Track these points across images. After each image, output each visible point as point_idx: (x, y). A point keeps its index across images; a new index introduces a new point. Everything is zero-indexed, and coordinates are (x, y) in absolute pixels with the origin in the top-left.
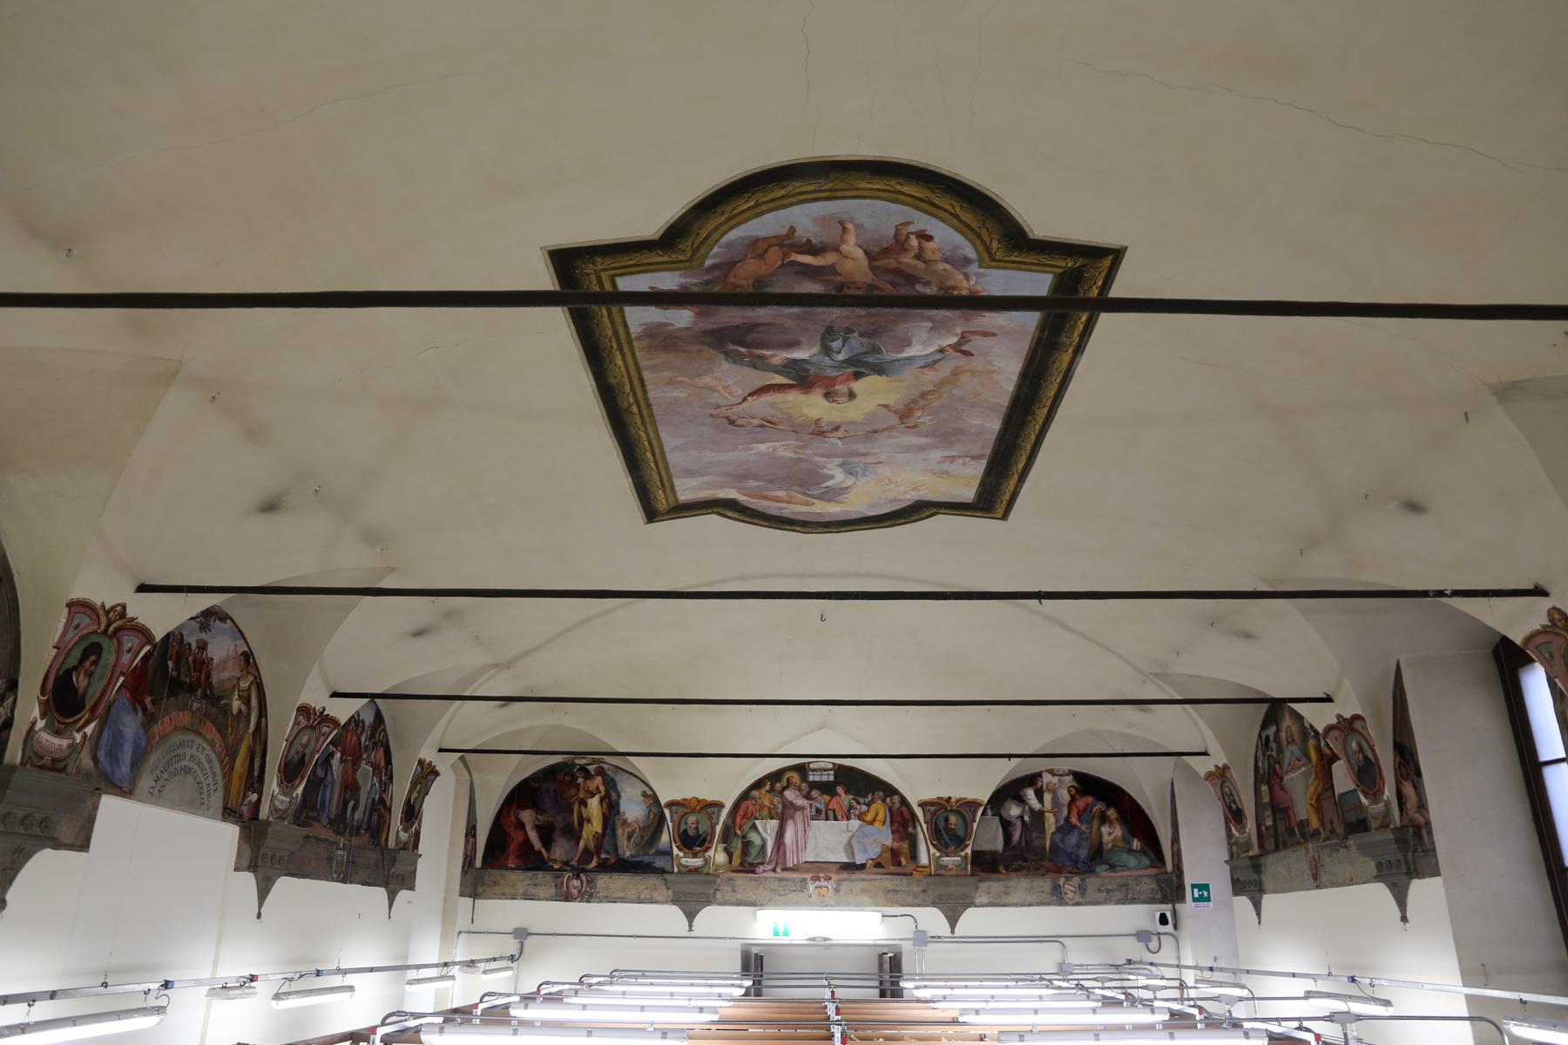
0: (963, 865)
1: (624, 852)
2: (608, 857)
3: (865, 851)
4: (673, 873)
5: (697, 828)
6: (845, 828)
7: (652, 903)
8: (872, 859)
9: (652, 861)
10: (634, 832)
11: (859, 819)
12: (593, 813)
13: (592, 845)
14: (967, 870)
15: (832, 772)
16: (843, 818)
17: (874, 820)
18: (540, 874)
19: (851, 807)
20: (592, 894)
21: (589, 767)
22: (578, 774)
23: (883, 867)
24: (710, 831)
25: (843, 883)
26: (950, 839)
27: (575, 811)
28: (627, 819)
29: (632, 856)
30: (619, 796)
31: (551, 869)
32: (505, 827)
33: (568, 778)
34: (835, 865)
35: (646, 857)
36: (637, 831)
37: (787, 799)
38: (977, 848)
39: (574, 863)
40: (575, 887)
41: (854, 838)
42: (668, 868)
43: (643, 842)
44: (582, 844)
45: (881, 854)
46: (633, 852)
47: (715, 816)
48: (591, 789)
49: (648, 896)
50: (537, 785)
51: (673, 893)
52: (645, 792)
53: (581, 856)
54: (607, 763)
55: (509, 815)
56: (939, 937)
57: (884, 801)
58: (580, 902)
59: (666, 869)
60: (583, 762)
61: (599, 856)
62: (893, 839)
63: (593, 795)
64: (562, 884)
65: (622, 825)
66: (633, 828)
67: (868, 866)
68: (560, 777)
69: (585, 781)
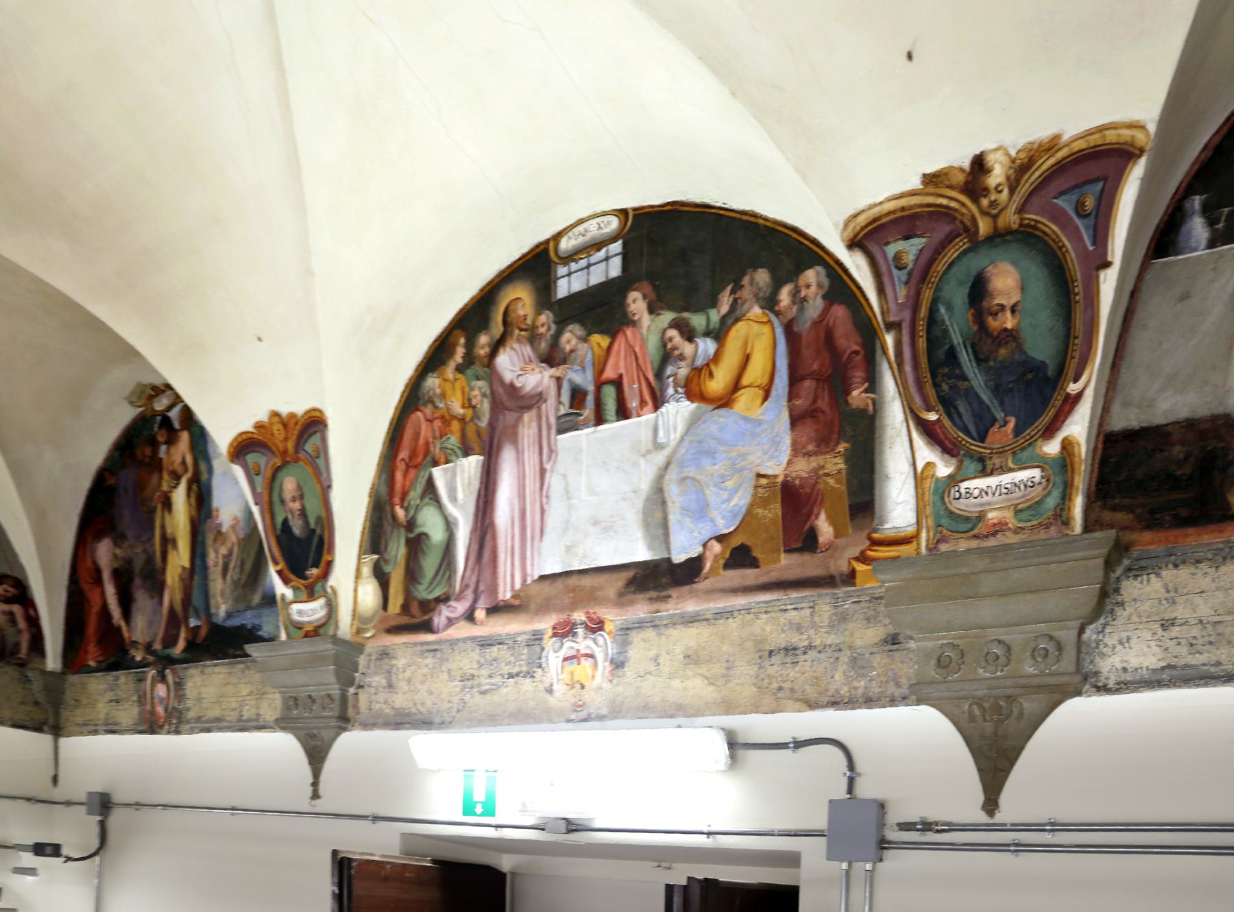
0: (1052, 502)
3: (701, 511)
6: (646, 436)
8: (720, 538)
11: (690, 396)
14: (1067, 523)
15: (617, 247)
16: (643, 403)
17: (736, 386)
19: (667, 356)
23: (754, 563)
25: (633, 633)
26: (997, 390)
34: (615, 576)
37: (501, 380)
38: (1122, 420)
41: (673, 469)
45: (749, 512)
56: (927, 826)
57: (770, 303)
62: (796, 450)
67: (708, 566)
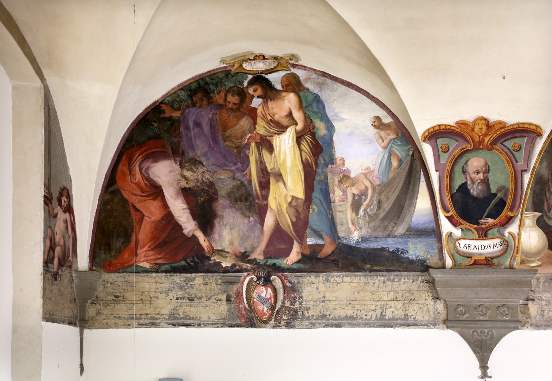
1: (350, 233)
2: (320, 242)
4: (444, 267)
5: (485, 182)
7: (408, 326)
9: (401, 247)
10: (364, 193)
12: (284, 160)
13: (287, 223)
18: (198, 278)
20: (296, 312)
21: (271, 77)
22: (251, 91)
24: (510, 185)
27: (253, 159)
28: (348, 171)
29: (364, 239)
30: (330, 128)
31: (216, 268)
32: (126, 195)
33: (233, 99)
35: (390, 240)
36: (370, 192)
39: (258, 255)
40: (264, 301)
42: (433, 260)
43: (382, 214)
44: (269, 221)
46: (365, 232)
47: (521, 156)
48: (277, 117)
49: (400, 313)
50: (176, 114)
51: (446, 307)
52: (378, 118)
53: (268, 245)
54: (304, 68)
55: (131, 171)
58: (274, 327)
59: (429, 263)
60: (259, 66)
61: (302, 239)
63: (282, 129)
64: (239, 294)
65: (340, 182)
66: (363, 188)
68: (219, 99)
69: (265, 103)
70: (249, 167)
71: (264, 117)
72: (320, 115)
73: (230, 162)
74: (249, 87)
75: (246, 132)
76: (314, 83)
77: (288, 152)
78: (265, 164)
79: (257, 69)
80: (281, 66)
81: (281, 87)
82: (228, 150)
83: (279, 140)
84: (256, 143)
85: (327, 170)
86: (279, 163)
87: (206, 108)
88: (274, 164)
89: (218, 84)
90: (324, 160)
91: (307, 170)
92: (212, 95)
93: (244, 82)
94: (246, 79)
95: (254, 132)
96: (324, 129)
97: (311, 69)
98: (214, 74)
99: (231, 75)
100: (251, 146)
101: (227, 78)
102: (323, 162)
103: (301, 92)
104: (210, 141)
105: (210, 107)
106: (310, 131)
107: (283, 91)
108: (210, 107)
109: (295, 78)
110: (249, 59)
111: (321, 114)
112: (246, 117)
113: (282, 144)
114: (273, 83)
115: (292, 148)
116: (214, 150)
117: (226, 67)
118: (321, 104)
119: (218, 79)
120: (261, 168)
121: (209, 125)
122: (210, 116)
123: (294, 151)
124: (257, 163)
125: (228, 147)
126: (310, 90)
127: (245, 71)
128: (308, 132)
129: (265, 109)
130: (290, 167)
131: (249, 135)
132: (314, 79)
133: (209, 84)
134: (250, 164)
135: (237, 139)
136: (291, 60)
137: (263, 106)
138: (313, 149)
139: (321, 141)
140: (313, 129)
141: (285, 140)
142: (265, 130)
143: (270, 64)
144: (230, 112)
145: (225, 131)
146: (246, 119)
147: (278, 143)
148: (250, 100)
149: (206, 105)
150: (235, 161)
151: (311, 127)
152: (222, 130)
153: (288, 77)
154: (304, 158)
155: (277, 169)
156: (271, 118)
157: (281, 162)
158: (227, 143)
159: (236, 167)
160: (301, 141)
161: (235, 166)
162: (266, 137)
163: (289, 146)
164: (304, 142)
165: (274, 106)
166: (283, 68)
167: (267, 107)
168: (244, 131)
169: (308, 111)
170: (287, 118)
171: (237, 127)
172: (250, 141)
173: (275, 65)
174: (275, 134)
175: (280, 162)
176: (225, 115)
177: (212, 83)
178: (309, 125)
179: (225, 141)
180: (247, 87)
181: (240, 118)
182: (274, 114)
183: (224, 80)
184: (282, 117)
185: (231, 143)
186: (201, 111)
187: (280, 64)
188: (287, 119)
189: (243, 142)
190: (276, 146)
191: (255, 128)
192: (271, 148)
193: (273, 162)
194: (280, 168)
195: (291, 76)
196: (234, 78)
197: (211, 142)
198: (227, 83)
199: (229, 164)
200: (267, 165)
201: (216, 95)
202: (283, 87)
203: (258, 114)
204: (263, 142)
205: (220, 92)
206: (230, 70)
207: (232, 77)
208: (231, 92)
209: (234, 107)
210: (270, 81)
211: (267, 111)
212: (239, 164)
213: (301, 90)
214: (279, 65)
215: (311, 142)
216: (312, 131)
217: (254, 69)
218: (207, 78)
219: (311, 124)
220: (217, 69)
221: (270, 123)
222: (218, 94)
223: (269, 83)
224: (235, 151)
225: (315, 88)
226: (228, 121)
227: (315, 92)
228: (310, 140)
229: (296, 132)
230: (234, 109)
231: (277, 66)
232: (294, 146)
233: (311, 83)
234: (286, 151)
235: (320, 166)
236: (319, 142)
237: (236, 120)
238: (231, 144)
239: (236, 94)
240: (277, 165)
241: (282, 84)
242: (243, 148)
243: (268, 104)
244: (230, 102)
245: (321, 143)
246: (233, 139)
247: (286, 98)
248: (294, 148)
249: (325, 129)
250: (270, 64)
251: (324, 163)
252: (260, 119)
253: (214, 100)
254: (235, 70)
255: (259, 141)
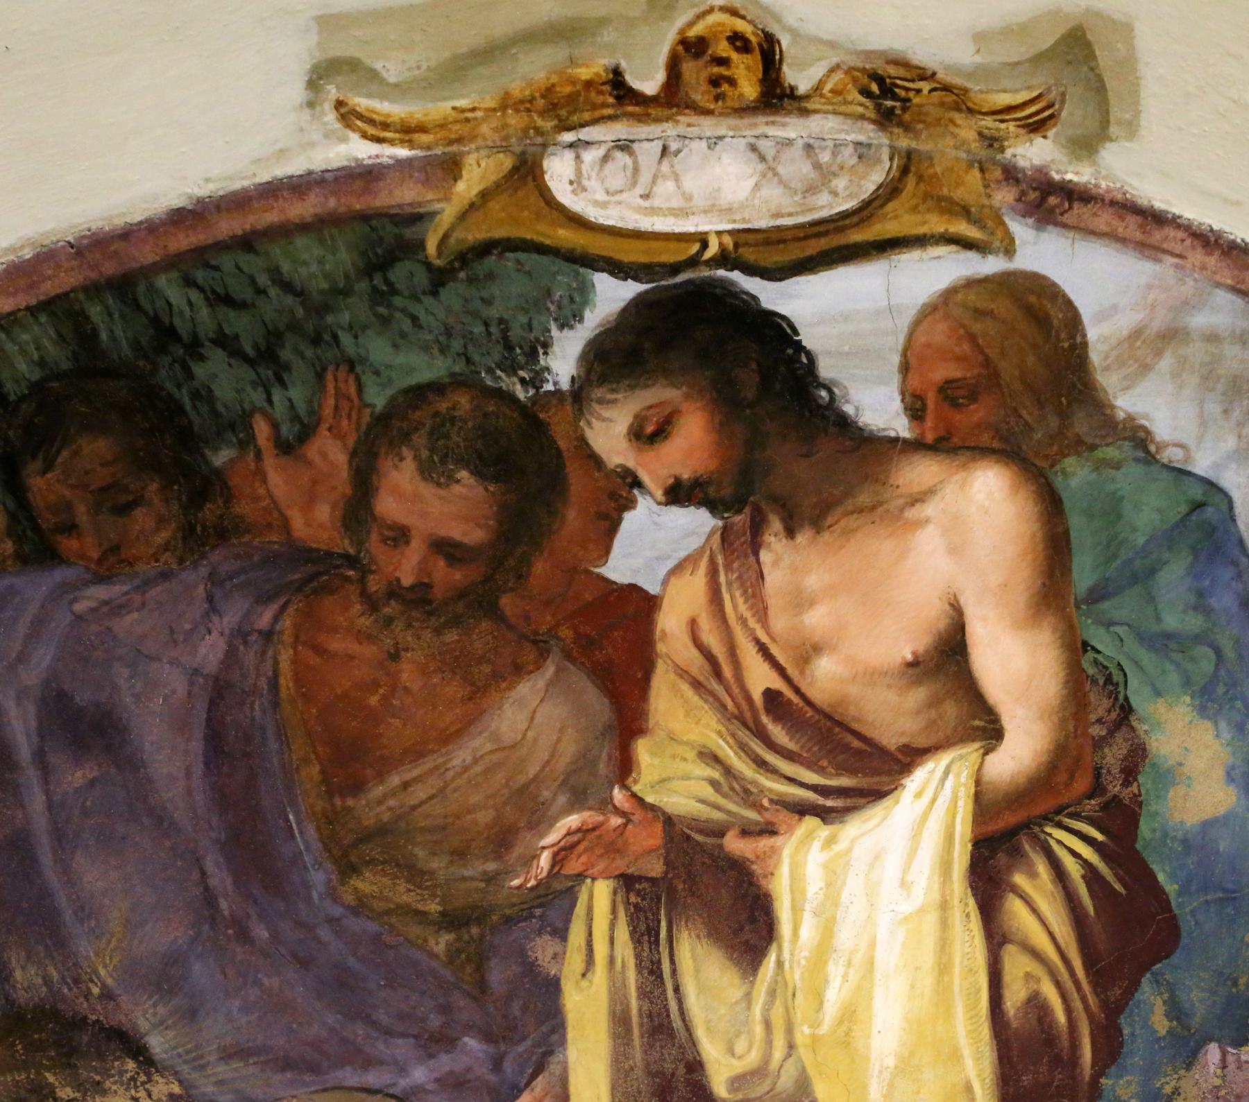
12: (851, 1015)
70: (554, 1067)
71: (717, 673)
72: (1207, 666)
73: (388, 1033)
74: (598, 393)
75: (546, 794)
76: (1208, 378)
77: (888, 957)
78: (694, 1043)
79: (683, 213)
80: (927, 196)
81: (897, 404)
82: (377, 938)
83: (826, 866)
84: (627, 882)
85: (1186, 1085)
86: (803, 1033)
87: (165, 576)
88: (769, 1042)
89: (286, 354)
90: (1176, 1011)
91: (1026, 1079)
92: (221, 457)
93: (546, 346)
94: (570, 318)
95: (618, 795)
96: (1220, 773)
97: (1208, 240)
98: (246, 243)
99: (428, 265)
100: (580, 909)
101: (379, 297)
102: (1161, 1024)
103: (1070, 462)
104: (209, 864)
105: (203, 571)
106: (1097, 789)
107: (916, 446)
108: (203, 571)
109: (1040, 319)
110: (617, 82)
111: (1218, 651)
112: (550, 670)
113: (853, 888)
114: (826, 370)
115: (931, 922)
116: (244, 936)
117: (366, 175)
118: (1227, 573)
119: (289, 300)
120: (650, 1074)
121: (199, 733)
122: (203, 651)
123: (944, 944)
124: (629, 1031)
125: (378, 916)
126: (1159, 448)
127: (565, 236)
128: (1079, 802)
129: (736, 605)
130: (891, 1062)
131: (573, 820)
132: (1213, 338)
133: (194, 348)
134: (563, 1042)
135: (460, 854)
136: (1036, 127)
137: (713, 572)
138: (1097, 928)
139: (1172, 877)
140: (1130, 772)
141: (877, 858)
142: (714, 783)
143: (825, 175)
144: (398, 626)
145: (357, 788)
146: (551, 684)
147: (814, 884)
148: (603, 516)
149: (166, 547)
150: (435, 1021)
151: (1113, 756)
152: (326, 779)
153: (979, 313)
154: (1014, 997)
155: (786, 1081)
156: (777, 684)
157: (825, 1029)
158: (366, 884)
159: (446, 1063)
160: (1010, 869)
161: (431, 1056)
162: (721, 834)
163: (906, 907)
164: (1033, 875)
165: (813, 581)
166: (937, 224)
167: (754, 583)
168: (522, 790)
169: (1109, 624)
170: (917, 682)
171: (461, 755)
172: (574, 866)
173: (874, 179)
174: (802, 810)
175: (816, 1024)
176: (355, 648)
177: (225, 341)
178: (1099, 744)
179: (348, 869)
180: (579, 395)
181: (497, 677)
182: (809, 651)
183: (345, 317)
184: (873, 676)
185: (402, 886)
186: (116, 609)
187: (920, 178)
188: (919, 695)
189: (510, 872)
190: (797, 910)
191: (625, 767)
192: (753, 920)
193: (759, 1030)
194: (811, 1071)
195: (1003, 307)
196: (453, 295)
197: (219, 877)
198: (378, 349)
199: (381, 1048)
200: (711, 1050)
201: (270, 463)
202: (915, 409)
203: (661, 647)
204: (691, 878)
205: (306, 432)
206: (418, 218)
207: (434, 293)
208: (420, 439)
209: (445, 576)
210: (799, 347)
211: (744, 621)
212: (472, 1043)
213: (1079, 446)
214: (911, 181)
215: (1091, 873)
216: (1115, 788)
217: (653, 211)
218: (170, 288)
219: (1119, 738)
220: (271, 191)
221: (765, 719)
222: (285, 448)
223: (794, 360)
224: (441, 943)
225: (1204, 423)
226: (384, 698)
227: (1202, 465)
228: (1086, 864)
229: (978, 797)
230: (438, 593)
231: (889, 191)
232: (944, 906)
233: (1175, 375)
234: (872, 945)
235: (1136, 1055)
236: (1161, 877)
237: (454, 689)
238: (403, 894)
239: (463, 462)
240: (791, 1047)
241: (915, 382)
242: (508, 921)
243: (764, 556)
244: (399, 536)
245: (1171, 888)
246: (420, 853)
247: (929, 510)
248: (944, 923)
249: (1230, 777)
250: (825, 175)
251: (1170, 1032)
252: (675, 690)
253: (243, 508)
254: (463, 216)
255: (655, 868)
